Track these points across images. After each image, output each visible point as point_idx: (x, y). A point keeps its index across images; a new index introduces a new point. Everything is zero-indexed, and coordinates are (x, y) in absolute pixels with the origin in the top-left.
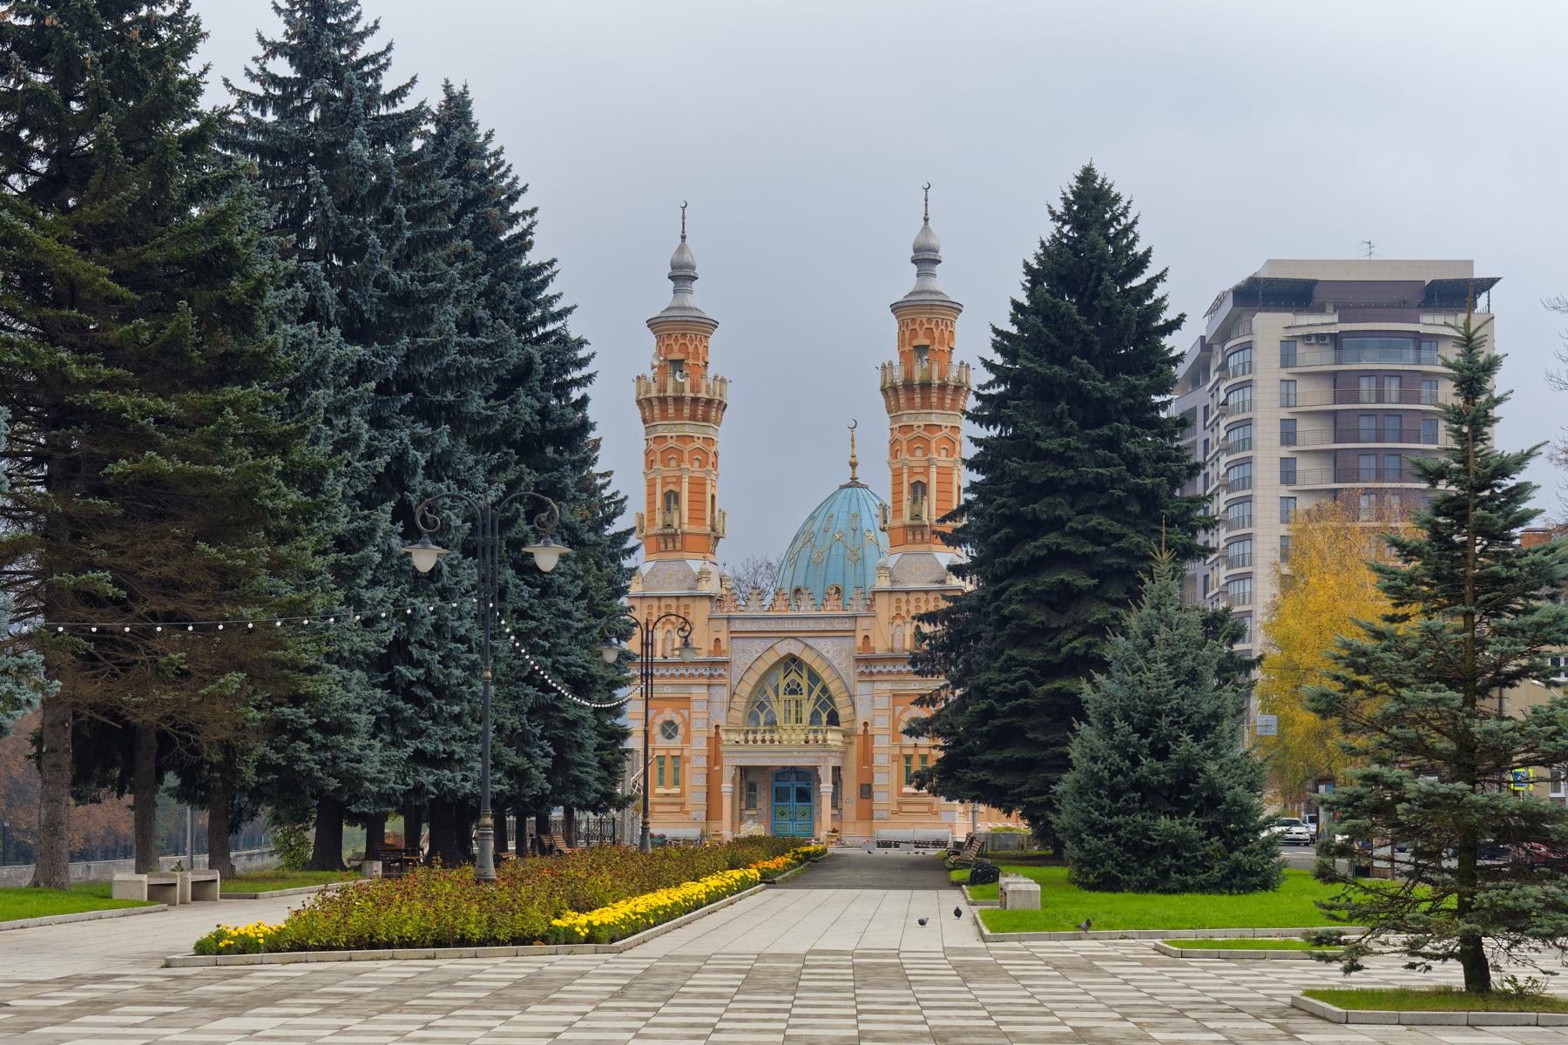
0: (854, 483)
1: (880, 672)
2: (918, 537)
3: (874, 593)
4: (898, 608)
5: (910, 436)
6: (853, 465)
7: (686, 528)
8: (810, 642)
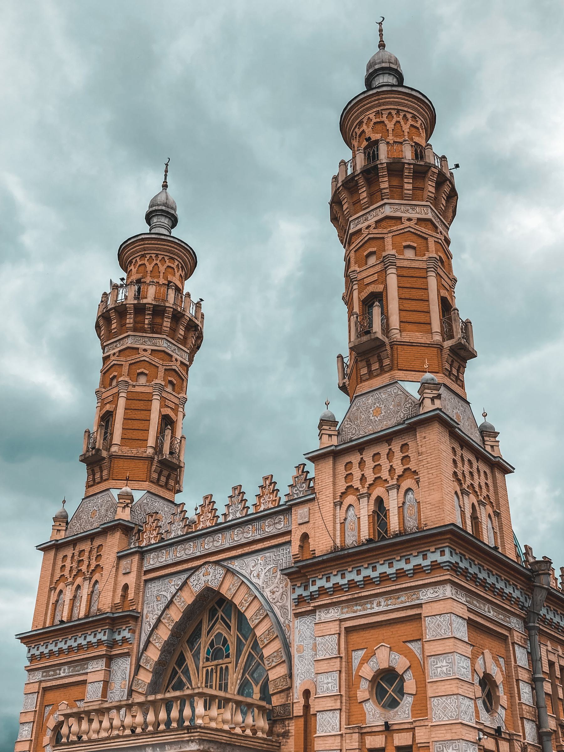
4: (349, 477)
8: (236, 565)
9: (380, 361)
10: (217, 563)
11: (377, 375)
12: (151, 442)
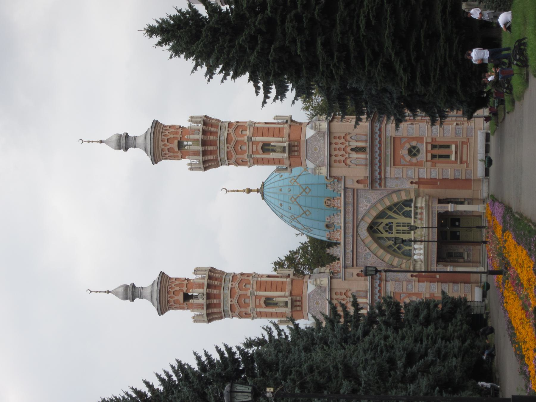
0: (261, 191)
1: (380, 173)
2: (296, 149)
3: (330, 176)
4: (340, 161)
5: (233, 153)
6: (249, 191)
7: (287, 294)
8: (360, 217)
9: (294, 146)
10: (357, 226)
11: (300, 148)
12: (285, 280)
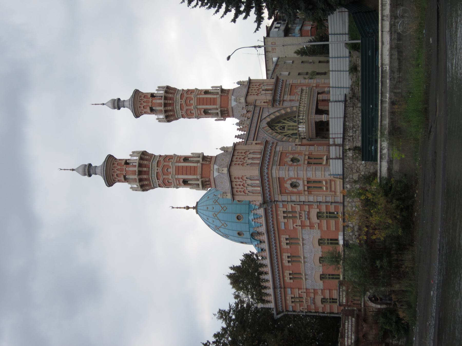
2: (208, 183)
6: (188, 208)
